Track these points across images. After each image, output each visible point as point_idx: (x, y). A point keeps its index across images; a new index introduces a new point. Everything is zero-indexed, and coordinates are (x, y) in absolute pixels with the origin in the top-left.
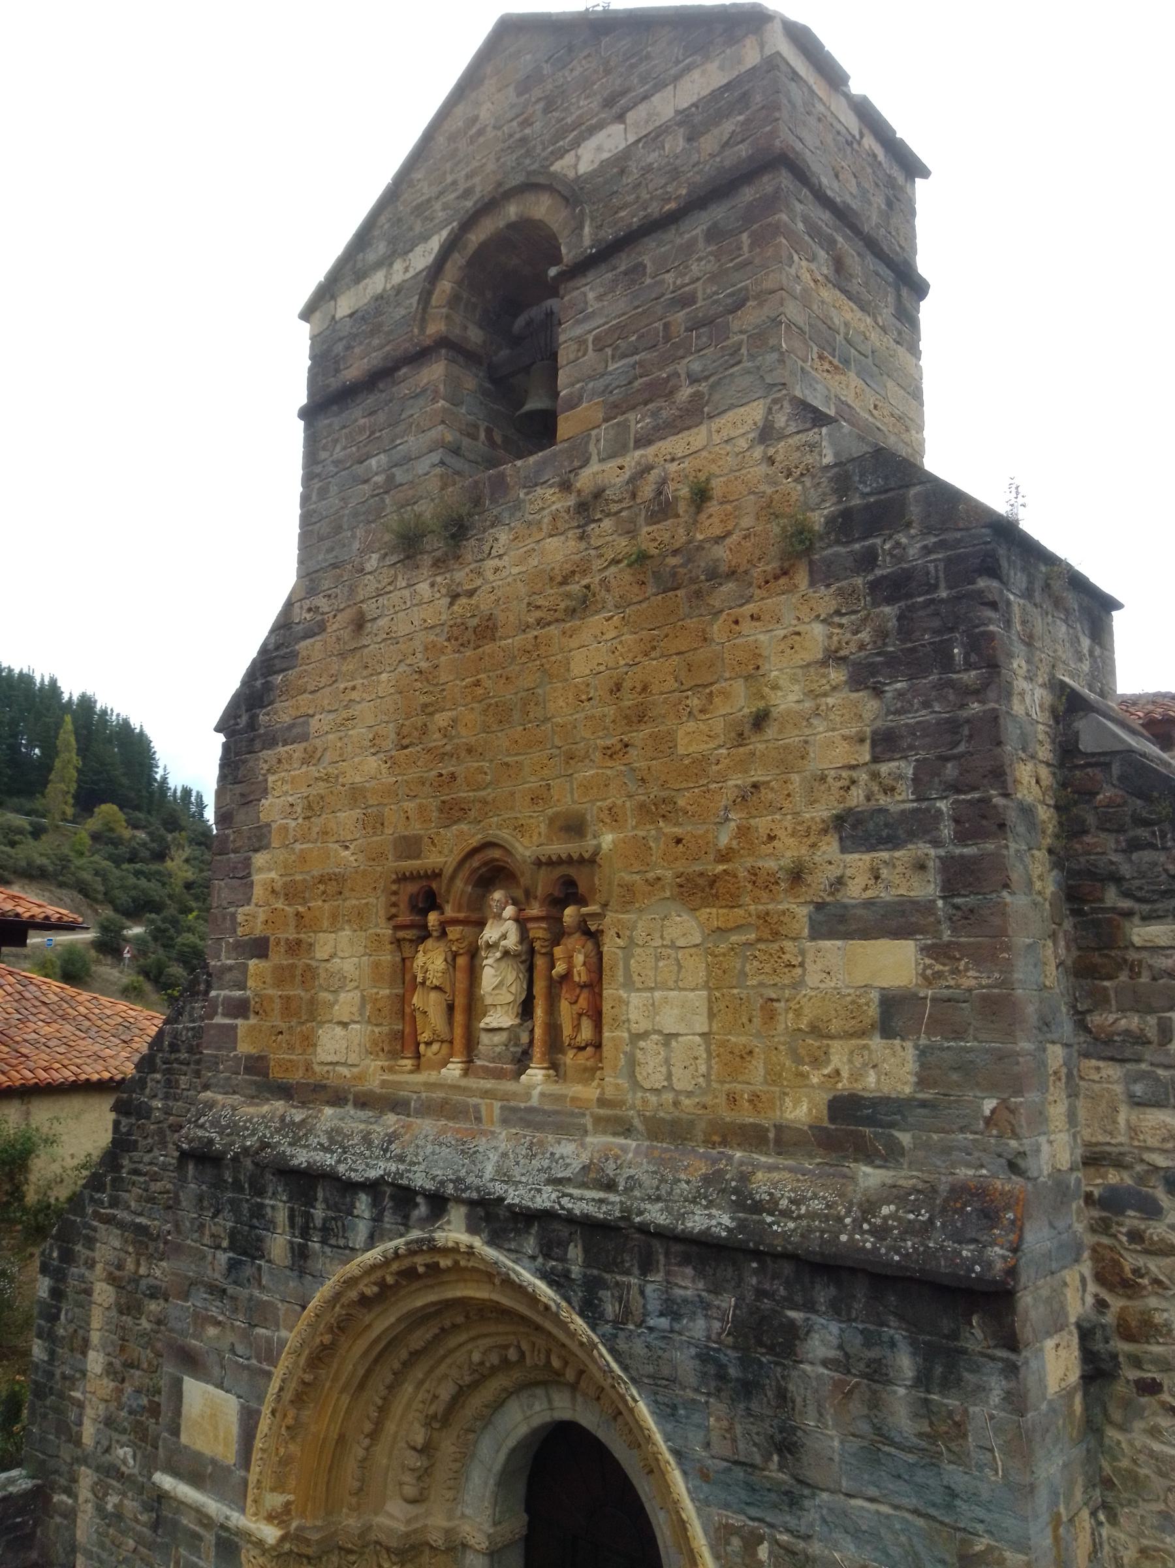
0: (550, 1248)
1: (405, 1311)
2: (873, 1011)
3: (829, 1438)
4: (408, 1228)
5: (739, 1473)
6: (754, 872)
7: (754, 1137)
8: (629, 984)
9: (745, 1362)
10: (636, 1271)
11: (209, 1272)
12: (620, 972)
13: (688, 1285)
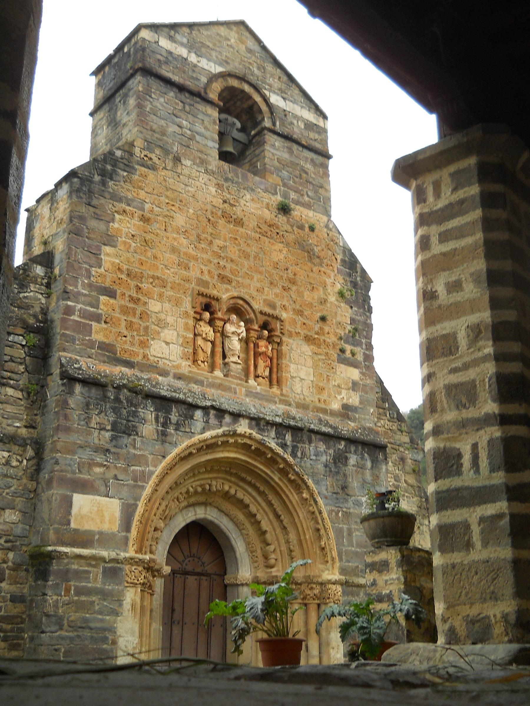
0: (279, 435)
1: (196, 463)
2: (351, 385)
4: (221, 426)
5: (335, 495)
6: (324, 341)
7: (325, 411)
8: (291, 362)
10: (307, 443)
12: (288, 357)
13: (322, 447)
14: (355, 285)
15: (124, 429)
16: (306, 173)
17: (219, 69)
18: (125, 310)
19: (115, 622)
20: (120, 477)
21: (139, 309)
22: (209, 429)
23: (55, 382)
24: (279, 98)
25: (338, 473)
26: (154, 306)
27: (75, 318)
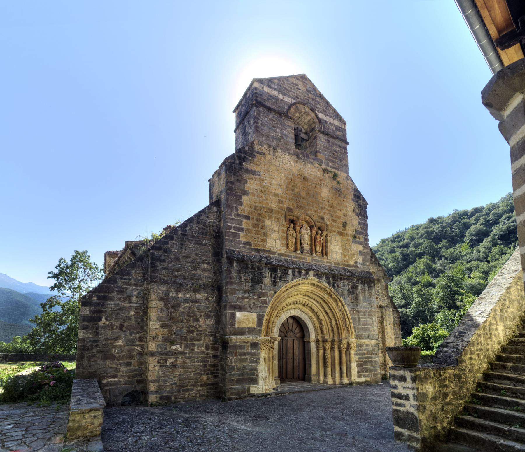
3: (361, 297)
7: (347, 265)
9: (352, 291)
11: (244, 288)
13: (346, 282)
14: (360, 206)
15: (257, 281)
16: (337, 152)
17: (293, 101)
18: (254, 226)
19: (257, 366)
20: (256, 303)
21: (261, 224)
22: (295, 278)
23: (225, 260)
24: (323, 115)
26: (268, 222)
27: (232, 230)
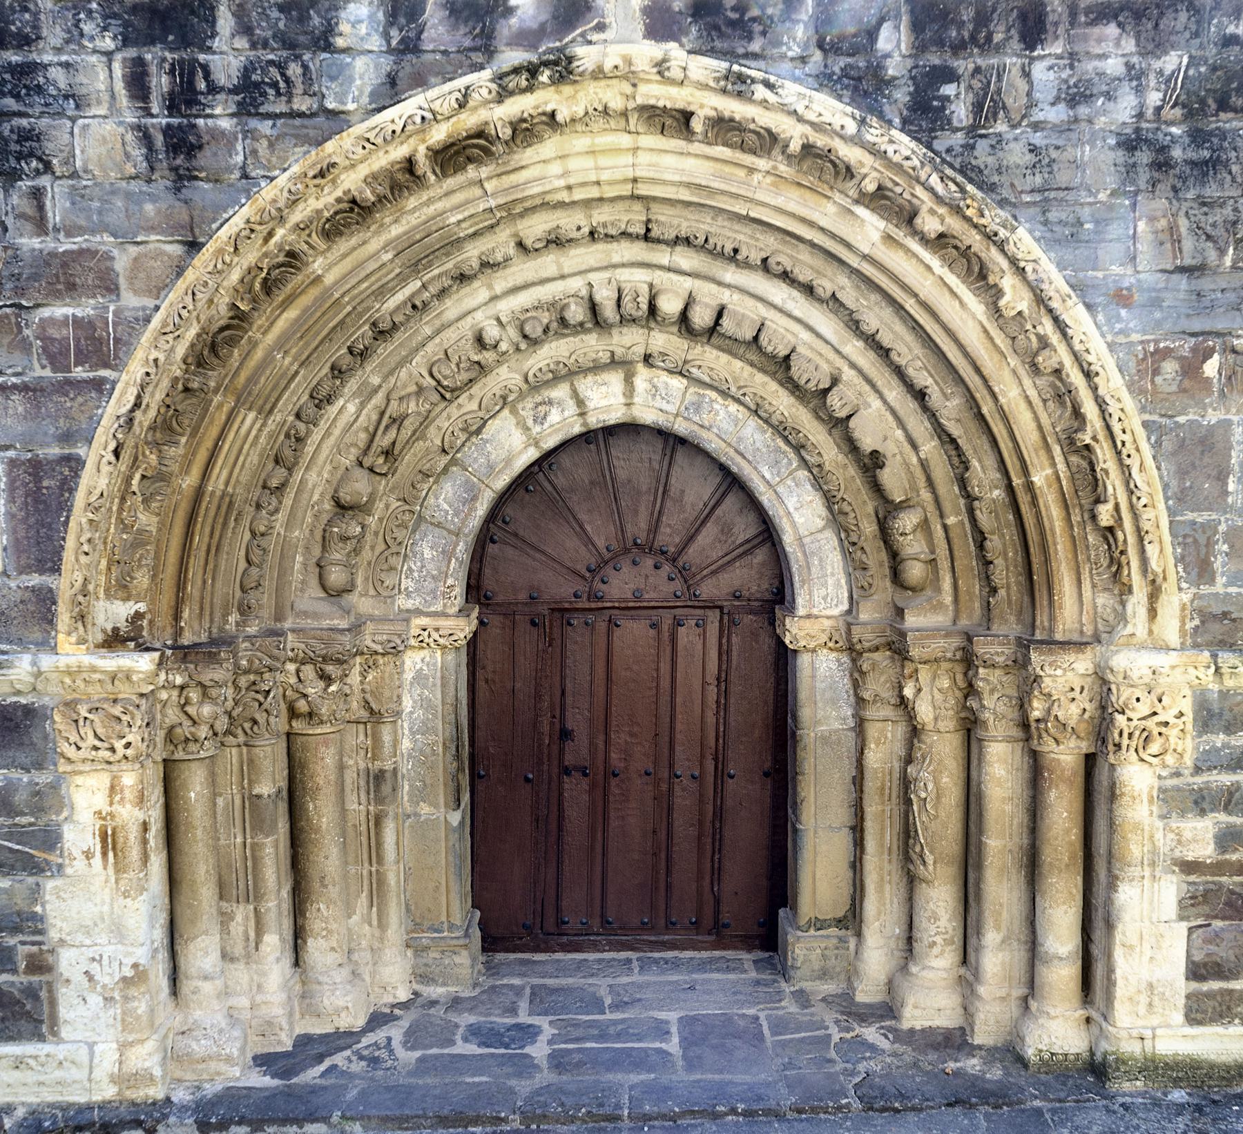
5: (1182, 282)
9: (1197, 137)
10: (1015, 45)
19: (35, 893)
22: (420, 81)
25: (1206, 168)
